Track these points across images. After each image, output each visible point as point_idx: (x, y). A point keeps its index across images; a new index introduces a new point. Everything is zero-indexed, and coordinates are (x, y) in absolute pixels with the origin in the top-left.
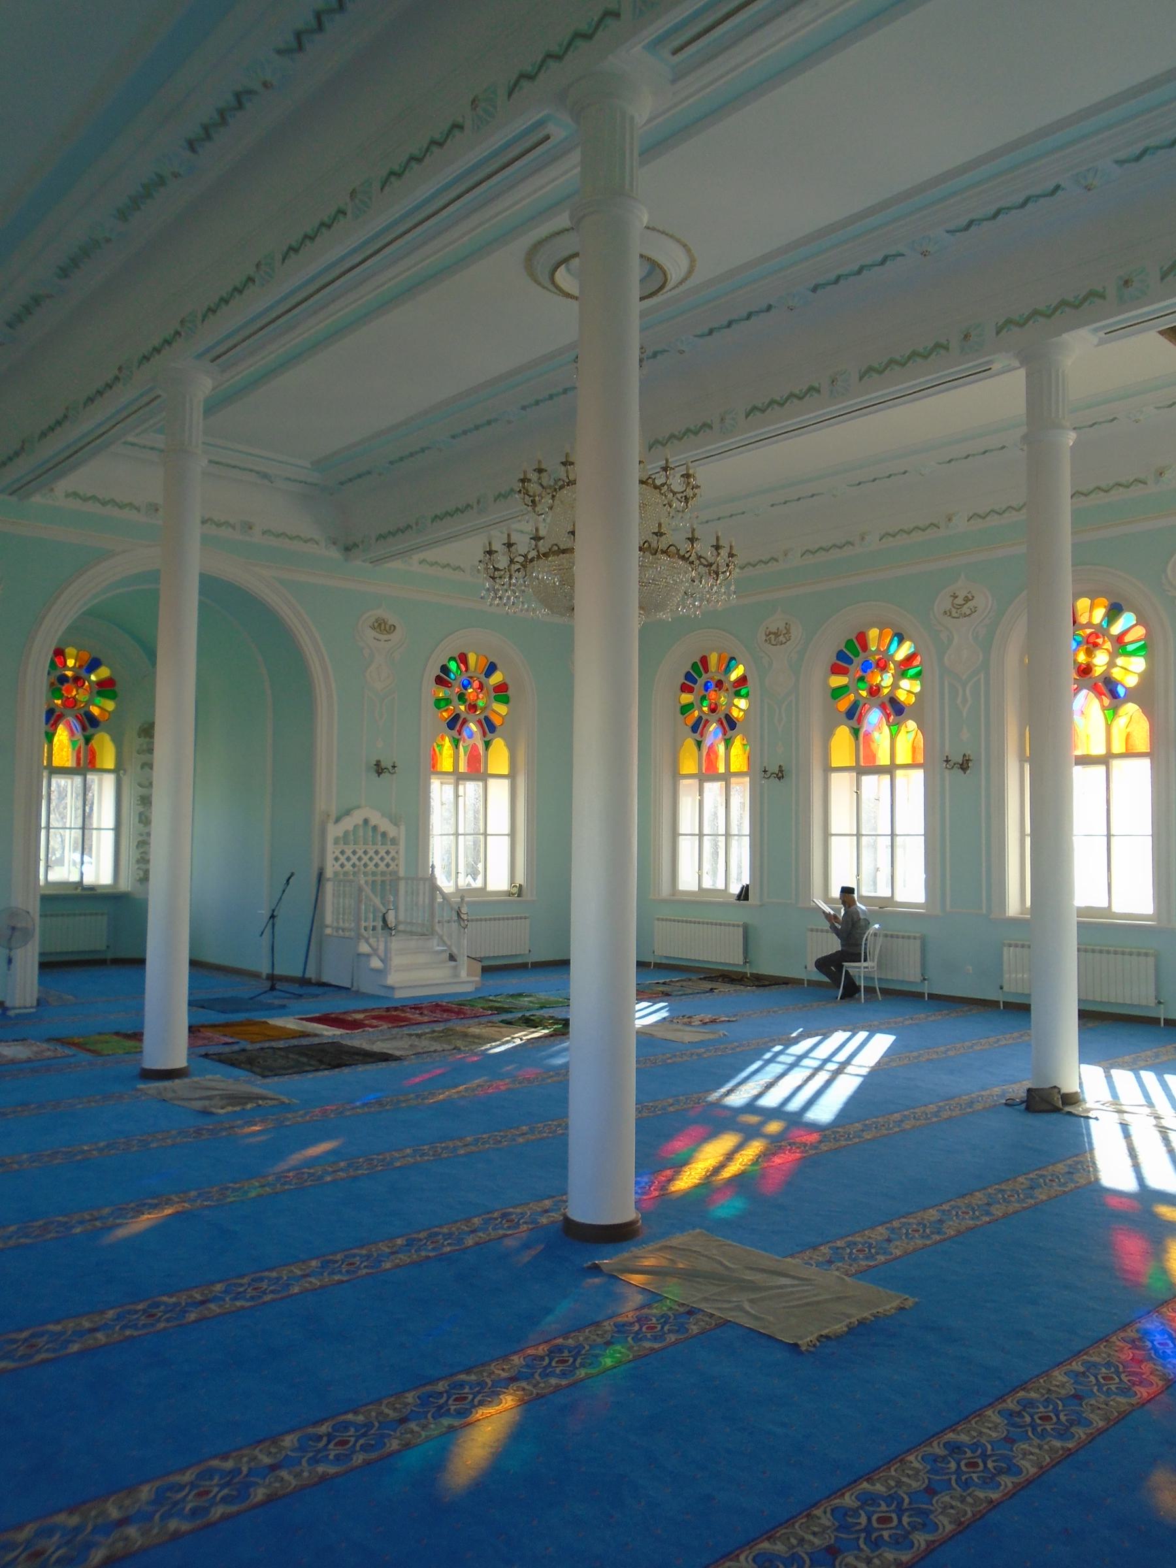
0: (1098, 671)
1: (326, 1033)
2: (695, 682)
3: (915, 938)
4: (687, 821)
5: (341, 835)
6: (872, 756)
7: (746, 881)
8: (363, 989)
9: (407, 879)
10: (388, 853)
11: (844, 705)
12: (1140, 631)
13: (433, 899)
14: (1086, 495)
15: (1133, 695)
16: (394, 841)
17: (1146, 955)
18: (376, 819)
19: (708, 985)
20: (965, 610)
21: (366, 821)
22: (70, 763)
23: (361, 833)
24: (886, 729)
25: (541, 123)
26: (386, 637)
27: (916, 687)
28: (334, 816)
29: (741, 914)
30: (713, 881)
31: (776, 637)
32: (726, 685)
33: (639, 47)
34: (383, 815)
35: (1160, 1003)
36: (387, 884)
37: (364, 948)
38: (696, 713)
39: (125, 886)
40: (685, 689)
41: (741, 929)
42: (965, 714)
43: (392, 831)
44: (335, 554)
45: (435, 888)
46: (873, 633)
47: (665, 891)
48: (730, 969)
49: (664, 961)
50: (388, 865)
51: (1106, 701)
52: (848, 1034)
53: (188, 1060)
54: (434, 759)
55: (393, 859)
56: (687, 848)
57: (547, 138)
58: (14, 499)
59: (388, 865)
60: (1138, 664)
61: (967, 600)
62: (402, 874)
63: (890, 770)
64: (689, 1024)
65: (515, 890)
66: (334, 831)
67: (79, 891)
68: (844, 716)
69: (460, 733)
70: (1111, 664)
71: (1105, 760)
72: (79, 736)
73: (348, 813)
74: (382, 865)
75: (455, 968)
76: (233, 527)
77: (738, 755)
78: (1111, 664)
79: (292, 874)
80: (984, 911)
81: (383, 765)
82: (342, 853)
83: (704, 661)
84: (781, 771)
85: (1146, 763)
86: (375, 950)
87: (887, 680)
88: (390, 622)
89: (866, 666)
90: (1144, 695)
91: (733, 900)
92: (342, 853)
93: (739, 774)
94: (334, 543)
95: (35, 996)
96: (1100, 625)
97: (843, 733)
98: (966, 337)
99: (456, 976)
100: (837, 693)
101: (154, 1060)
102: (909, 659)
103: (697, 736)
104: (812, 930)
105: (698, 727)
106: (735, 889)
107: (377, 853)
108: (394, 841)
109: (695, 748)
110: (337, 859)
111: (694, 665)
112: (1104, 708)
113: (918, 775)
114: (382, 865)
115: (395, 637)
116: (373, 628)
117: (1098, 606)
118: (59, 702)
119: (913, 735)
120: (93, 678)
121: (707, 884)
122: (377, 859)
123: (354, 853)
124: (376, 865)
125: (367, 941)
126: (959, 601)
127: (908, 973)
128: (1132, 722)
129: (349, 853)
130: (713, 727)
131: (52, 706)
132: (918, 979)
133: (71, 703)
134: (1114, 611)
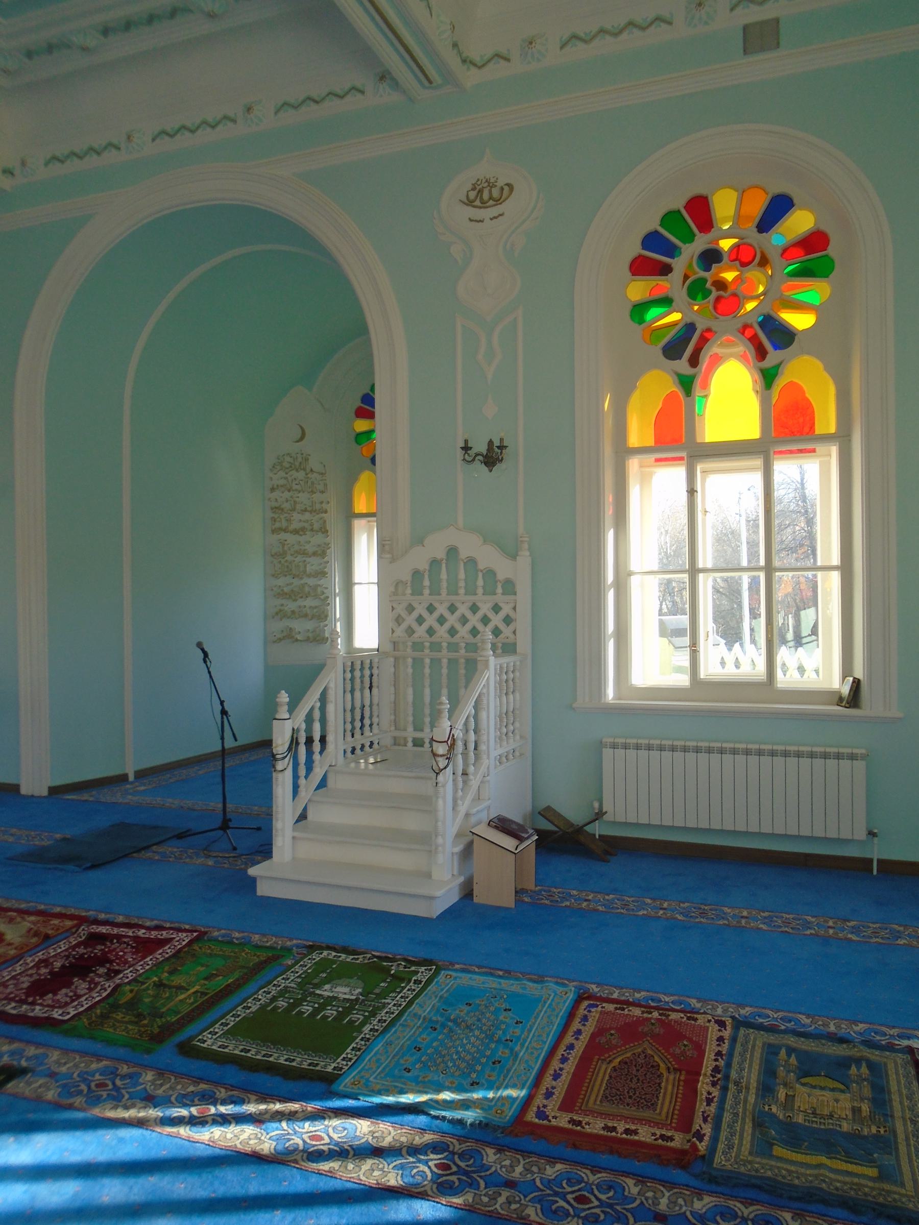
5: (407, 577)
10: (496, 609)
21: (452, 552)
23: (444, 576)
26: (494, 211)
34: (485, 542)
43: (504, 569)
55: (508, 620)
65: (846, 690)
69: (694, 361)
82: (410, 609)
88: (500, 183)
92: (410, 609)
107: (474, 609)
108: (509, 587)
110: (508, 620)
116: (469, 203)
123: (431, 609)
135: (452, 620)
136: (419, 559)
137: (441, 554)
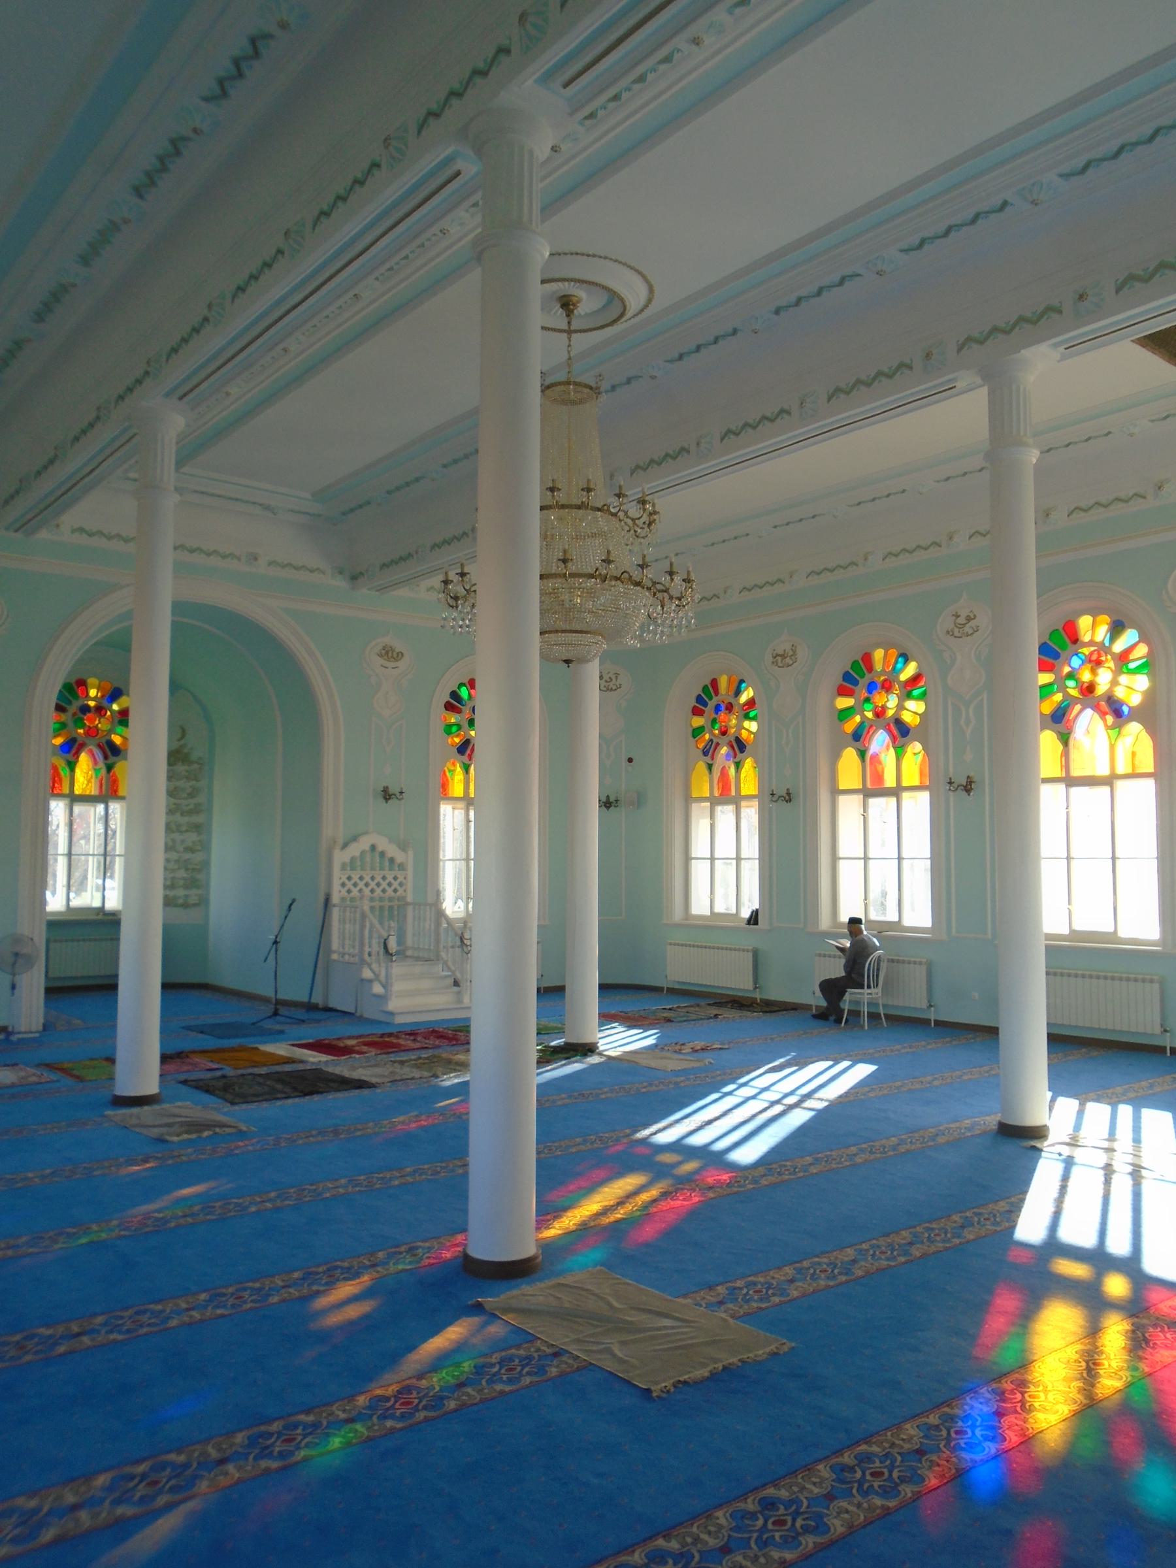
0: (1101, 690)
1: (311, 1059)
2: (706, 705)
3: (920, 963)
4: (700, 845)
6: (879, 777)
7: (756, 906)
8: (366, 1015)
9: (414, 904)
10: (395, 878)
11: (849, 727)
12: (1142, 650)
13: (438, 924)
14: (1085, 511)
15: (1138, 714)
16: (402, 867)
17: (1152, 981)
18: (383, 844)
19: (714, 1011)
20: (967, 629)
21: (373, 847)
22: (93, 790)
23: (368, 859)
24: (892, 750)
25: (449, 160)
27: (920, 707)
28: (341, 842)
29: (752, 939)
30: (725, 904)
31: (782, 659)
32: (736, 708)
33: (530, 82)
35: (1165, 1031)
36: (394, 910)
37: (367, 974)
38: (707, 737)
40: (697, 712)
41: (750, 954)
42: (968, 734)
43: (400, 857)
44: (341, 583)
45: (440, 914)
46: (878, 655)
47: (678, 916)
48: (740, 994)
49: (677, 986)
50: (395, 891)
51: (1110, 719)
52: (831, 1063)
53: (160, 1087)
54: (444, 785)
55: (401, 884)
56: (700, 872)
57: (458, 174)
58: (19, 535)
59: (395, 891)
60: (1142, 682)
61: (969, 619)
62: (409, 899)
63: (896, 792)
64: (679, 1052)
66: (341, 857)
67: (100, 917)
68: (850, 738)
70: (1114, 683)
71: (1108, 781)
72: (101, 764)
73: (355, 839)
74: (390, 891)
75: (459, 993)
76: (239, 559)
77: (748, 779)
78: (1114, 683)
79: (294, 901)
80: (990, 936)
81: (391, 791)
82: (349, 878)
83: (714, 683)
84: (789, 794)
85: (1150, 784)
86: (377, 976)
87: (892, 702)
89: (871, 687)
90: (1147, 714)
91: (743, 924)
92: (349, 878)
93: (749, 797)
94: (340, 573)
95: (42, 1021)
96: (1102, 643)
97: (850, 756)
98: (928, 356)
99: (460, 1001)
100: (845, 713)
101: (126, 1087)
102: (915, 680)
103: (708, 759)
104: (820, 955)
105: (709, 751)
106: (746, 914)
107: (384, 878)
108: (402, 867)
109: (706, 771)
111: (705, 688)
112: (1107, 727)
113: (925, 796)
114: (390, 891)
115: (402, 664)
116: (381, 656)
117: (1101, 623)
118: (81, 731)
119: (920, 756)
120: (115, 707)
121: (720, 908)
122: (384, 884)
123: (361, 878)
124: (384, 891)
125: (369, 965)
126: (962, 620)
127: (913, 1000)
128: (1136, 741)
129: (355, 878)
130: (724, 750)
131: (74, 735)
132: (924, 1005)
133: (92, 732)
134: (1117, 628)
135: (373, 885)
136: (355, 850)
137: (367, 847)
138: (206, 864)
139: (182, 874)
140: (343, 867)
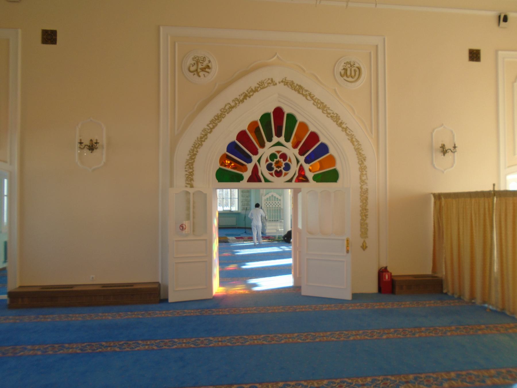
16: (280, 200)
18: (275, 195)
21: (272, 196)
39: (240, 211)
43: (279, 198)
62: (282, 208)
66: (264, 198)
74: (277, 206)
108: (280, 200)
114: (277, 206)
136: (268, 196)
138: (250, 201)
139: (246, 202)
140: (265, 200)
